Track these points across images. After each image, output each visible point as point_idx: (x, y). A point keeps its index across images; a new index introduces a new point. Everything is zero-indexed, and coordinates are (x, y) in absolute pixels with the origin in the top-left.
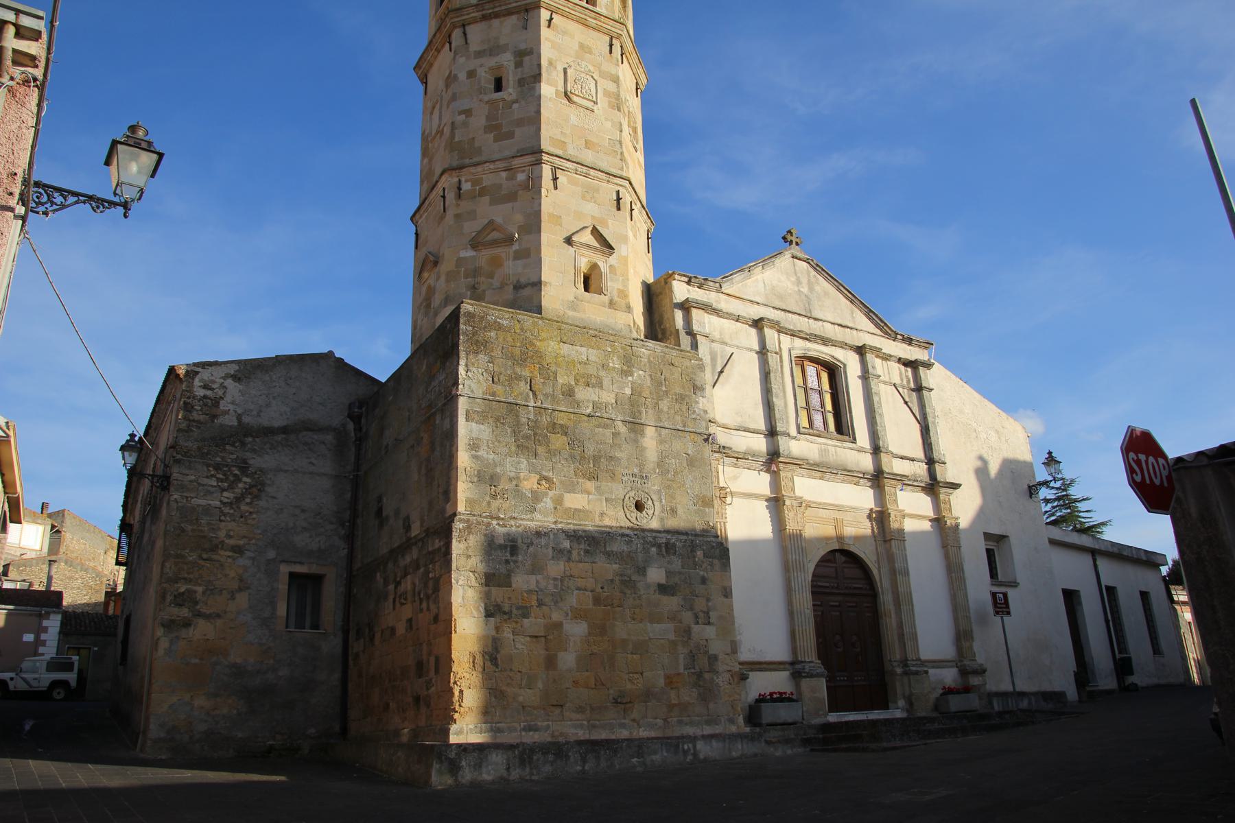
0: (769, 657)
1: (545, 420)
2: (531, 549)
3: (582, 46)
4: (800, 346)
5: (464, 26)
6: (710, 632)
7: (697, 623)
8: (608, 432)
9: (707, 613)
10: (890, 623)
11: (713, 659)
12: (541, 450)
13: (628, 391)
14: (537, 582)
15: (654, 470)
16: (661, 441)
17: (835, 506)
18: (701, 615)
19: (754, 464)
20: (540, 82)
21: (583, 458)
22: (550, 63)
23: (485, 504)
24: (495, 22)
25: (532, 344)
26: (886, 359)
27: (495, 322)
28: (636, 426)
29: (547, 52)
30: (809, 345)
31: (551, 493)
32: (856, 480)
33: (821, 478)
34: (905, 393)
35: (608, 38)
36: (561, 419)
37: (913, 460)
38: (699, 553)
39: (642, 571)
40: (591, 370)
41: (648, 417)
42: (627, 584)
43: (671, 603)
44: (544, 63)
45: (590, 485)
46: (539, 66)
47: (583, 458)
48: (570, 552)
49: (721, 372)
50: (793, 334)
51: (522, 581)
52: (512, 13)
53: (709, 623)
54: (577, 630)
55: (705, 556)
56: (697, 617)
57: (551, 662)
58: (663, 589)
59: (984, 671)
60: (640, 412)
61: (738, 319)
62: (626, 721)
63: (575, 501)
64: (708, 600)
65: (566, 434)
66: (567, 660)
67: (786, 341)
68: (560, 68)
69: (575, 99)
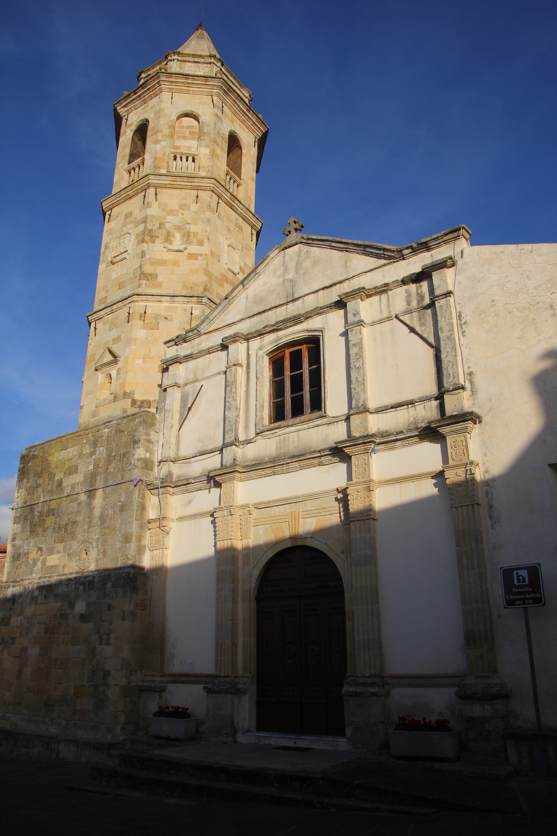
0: (198, 670)
1: (46, 508)
2: (21, 599)
4: (270, 341)
6: (108, 651)
7: (101, 643)
8: (75, 505)
9: (108, 635)
10: (357, 630)
11: (107, 674)
12: (41, 529)
13: (91, 467)
14: (21, 621)
15: (97, 522)
16: (105, 498)
17: (290, 500)
18: (105, 637)
19: (200, 485)
21: (60, 528)
23: (13, 574)
25: (47, 460)
26: (384, 291)
27: (33, 455)
28: (91, 493)
30: (281, 333)
31: (41, 558)
32: (316, 461)
33: (274, 474)
34: (413, 320)
36: (53, 505)
37: (412, 403)
38: (109, 585)
39: (72, 605)
40: (74, 462)
41: (99, 483)
42: (64, 616)
43: (87, 628)
45: (60, 546)
47: (60, 528)
48: (37, 598)
49: (190, 409)
50: (260, 334)
51: (16, 621)
53: (108, 644)
54: (34, 651)
55: (113, 586)
56: (101, 638)
57: (20, 673)
58: (83, 618)
59: (507, 697)
60: (96, 480)
61: (209, 351)
62: (47, 719)
63: (53, 560)
64: (111, 624)
65: (53, 515)
66: (28, 672)
67: (255, 344)
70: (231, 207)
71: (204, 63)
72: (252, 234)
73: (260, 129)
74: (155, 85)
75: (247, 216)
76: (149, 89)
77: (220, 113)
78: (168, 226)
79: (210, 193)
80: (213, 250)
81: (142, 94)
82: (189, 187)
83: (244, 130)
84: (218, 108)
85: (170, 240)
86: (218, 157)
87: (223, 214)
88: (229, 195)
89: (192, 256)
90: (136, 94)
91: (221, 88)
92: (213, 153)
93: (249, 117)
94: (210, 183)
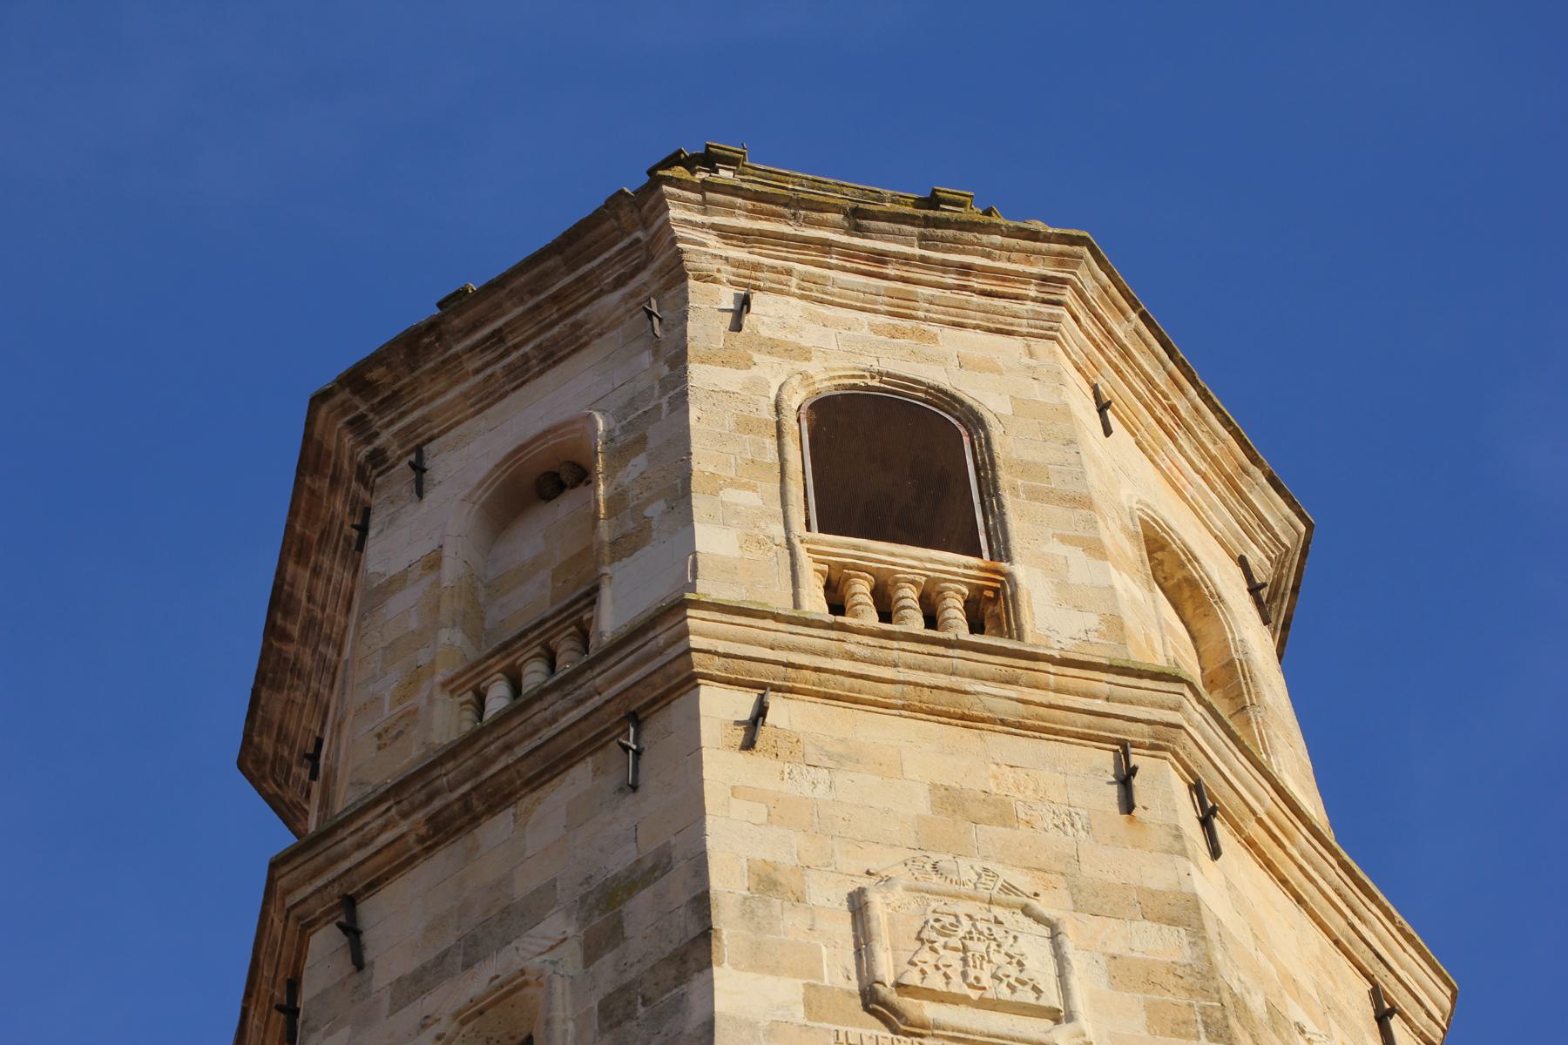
3: (949, 800)
5: (350, 903)
20: (706, 964)
22: (766, 882)
24: (496, 829)
29: (734, 841)
35: (1104, 759)
44: (726, 881)
46: (702, 903)
52: (568, 760)
68: (829, 896)
69: (930, 1011)
74: (1024, 278)
76: (965, 270)
81: (906, 260)
90: (858, 230)
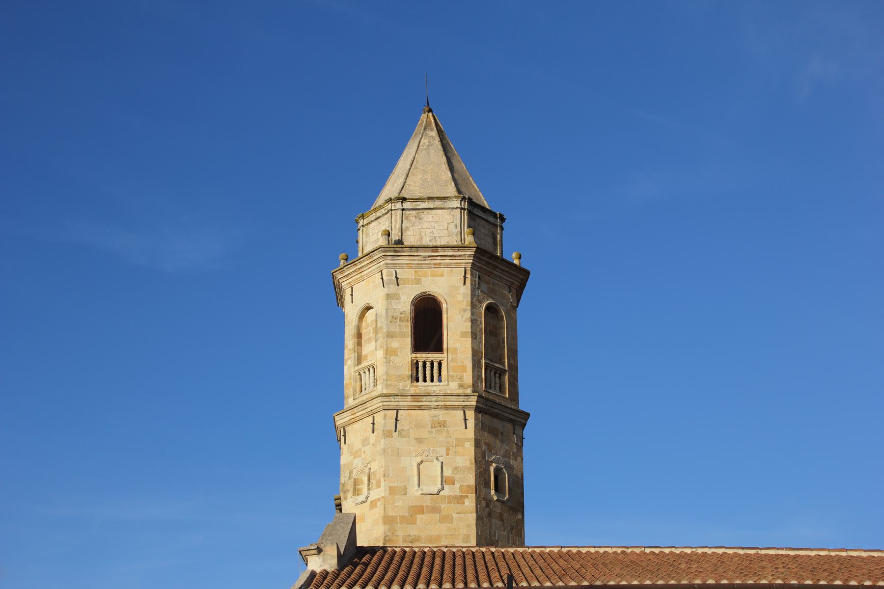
70: (420, 408)
71: (384, 215)
72: (465, 420)
73: (465, 255)
75: (448, 403)
77: (393, 288)
78: (355, 471)
79: (383, 412)
80: (394, 485)
82: (366, 415)
83: (442, 275)
84: (390, 283)
85: (359, 490)
86: (395, 352)
87: (406, 427)
88: (409, 398)
89: (373, 504)
91: (385, 256)
92: (389, 352)
93: (441, 256)
94: (377, 404)
